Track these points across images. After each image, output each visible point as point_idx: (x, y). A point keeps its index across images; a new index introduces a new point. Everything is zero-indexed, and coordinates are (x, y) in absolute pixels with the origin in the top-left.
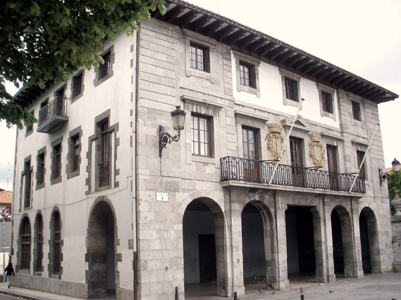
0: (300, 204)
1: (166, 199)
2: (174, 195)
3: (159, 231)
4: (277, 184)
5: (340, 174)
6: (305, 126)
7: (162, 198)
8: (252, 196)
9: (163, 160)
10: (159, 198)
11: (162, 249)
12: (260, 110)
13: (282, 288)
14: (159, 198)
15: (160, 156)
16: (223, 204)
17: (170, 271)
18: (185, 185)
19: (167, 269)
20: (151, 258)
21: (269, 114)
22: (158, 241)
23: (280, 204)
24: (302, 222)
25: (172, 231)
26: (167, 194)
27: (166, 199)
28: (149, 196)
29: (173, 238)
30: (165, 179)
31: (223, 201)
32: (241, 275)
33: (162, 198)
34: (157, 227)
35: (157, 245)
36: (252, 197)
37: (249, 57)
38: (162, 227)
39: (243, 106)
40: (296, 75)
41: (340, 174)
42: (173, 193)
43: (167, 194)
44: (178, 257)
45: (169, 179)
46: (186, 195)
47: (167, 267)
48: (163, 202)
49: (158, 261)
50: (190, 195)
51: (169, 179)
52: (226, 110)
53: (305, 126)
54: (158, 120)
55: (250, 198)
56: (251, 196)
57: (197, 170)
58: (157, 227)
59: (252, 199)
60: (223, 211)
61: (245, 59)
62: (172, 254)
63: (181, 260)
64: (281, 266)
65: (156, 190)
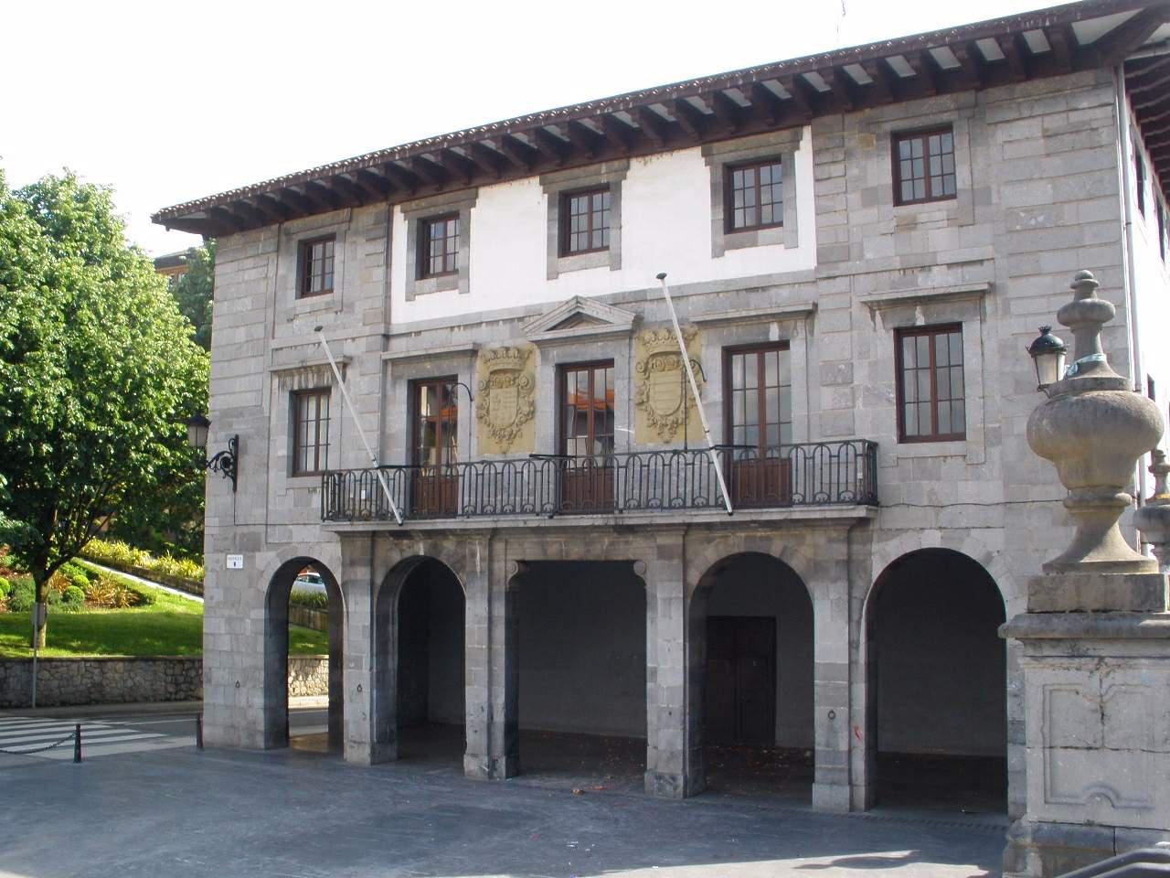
0: (564, 558)
1: (240, 565)
2: (254, 557)
3: (229, 620)
4: (518, 513)
5: (459, 464)
6: (1143, 212)
7: (235, 564)
8: (410, 548)
9: (238, 496)
10: (230, 565)
11: (232, 651)
12: (466, 326)
13: (471, 772)
14: (230, 565)
15: (235, 489)
16: (340, 570)
17: (243, 690)
18: (276, 536)
19: (238, 685)
20: (217, 665)
21: (495, 327)
22: (227, 638)
23: (478, 563)
24: (748, 627)
25: (248, 621)
26: (242, 556)
27: (240, 565)
28: (218, 561)
29: (248, 633)
30: (240, 530)
31: (339, 563)
32: (364, 719)
33: (235, 564)
34: (227, 612)
35: (225, 643)
36: (407, 550)
37: (440, 198)
38: (233, 613)
39: (418, 333)
40: (604, 168)
41: (459, 464)
42: (251, 554)
43: (242, 556)
44: (256, 668)
45: (245, 530)
46: (272, 554)
47: (238, 682)
48: (236, 569)
49: (227, 670)
50: (278, 555)
51: (245, 530)
52: (361, 363)
53: (1143, 212)
54: (235, 426)
55: (402, 551)
56: (404, 547)
57: (295, 505)
58: (227, 612)
59: (408, 554)
60: (339, 583)
61: (432, 209)
62: (247, 662)
63: (260, 673)
64: (472, 718)
65: (227, 551)
